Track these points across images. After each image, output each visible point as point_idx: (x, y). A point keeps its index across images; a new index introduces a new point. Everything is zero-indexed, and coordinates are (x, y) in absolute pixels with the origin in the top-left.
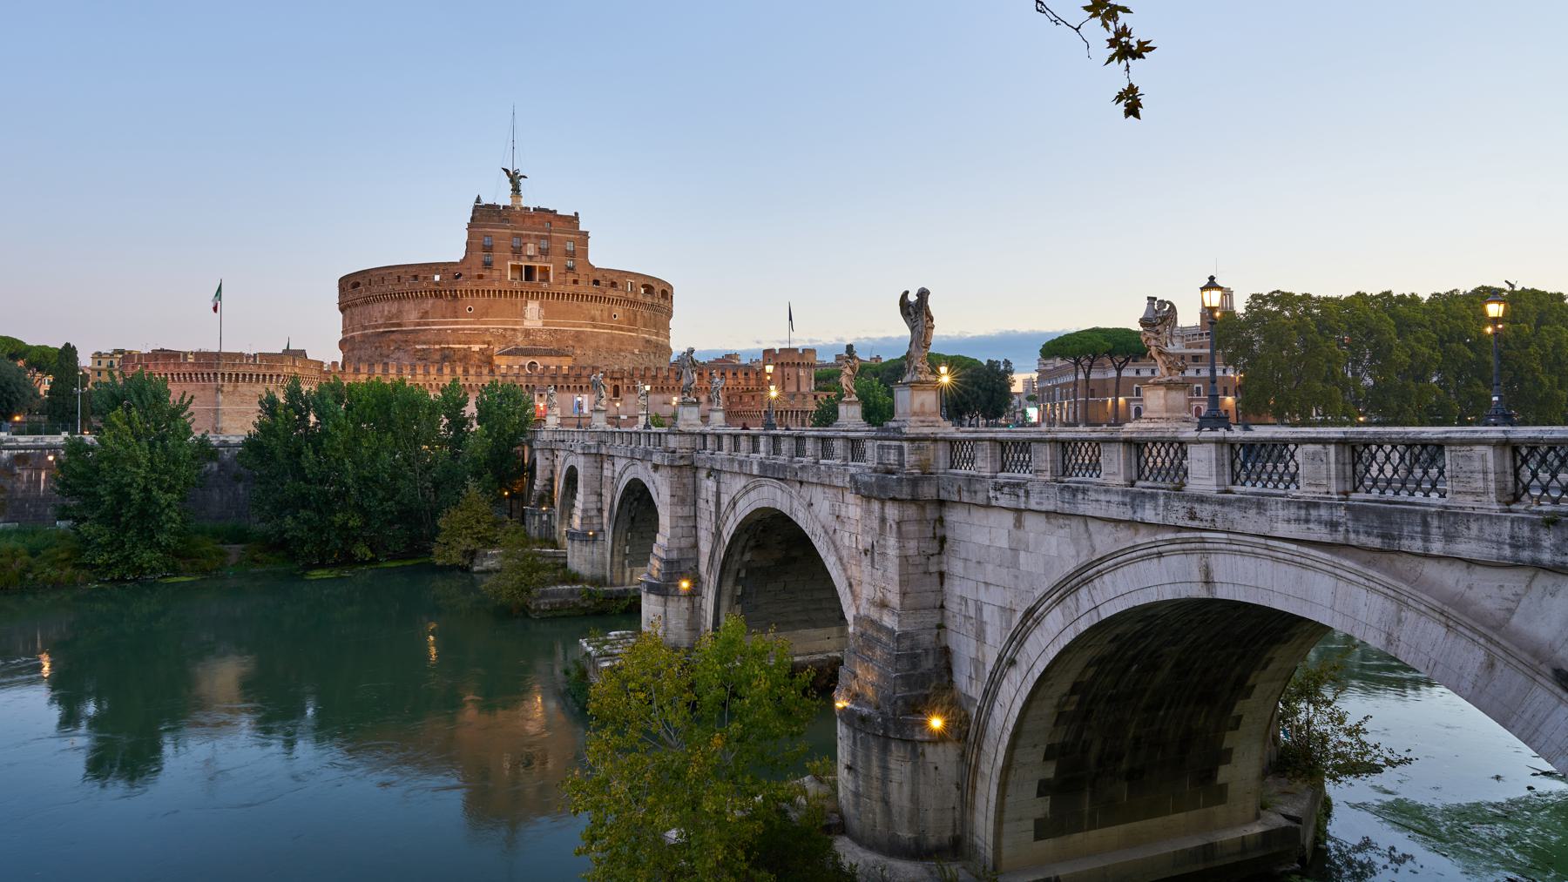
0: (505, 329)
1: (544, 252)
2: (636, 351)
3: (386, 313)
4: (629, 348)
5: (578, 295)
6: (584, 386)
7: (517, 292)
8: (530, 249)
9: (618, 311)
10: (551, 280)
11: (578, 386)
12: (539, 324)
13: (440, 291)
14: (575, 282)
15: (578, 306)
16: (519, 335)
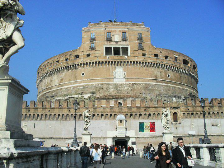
0: (103, 84)
1: (124, 39)
2: (183, 97)
3: (46, 83)
4: (179, 95)
5: (146, 63)
6: (152, 114)
7: (109, 62)
8: (117, 38)
9: (170, 73)
10: (129, 54)
11: (147, 114)
12: (123, 81)
13: (68, 66)
14: (144, 55)
15: (146, 69)
16: (111, 87)
